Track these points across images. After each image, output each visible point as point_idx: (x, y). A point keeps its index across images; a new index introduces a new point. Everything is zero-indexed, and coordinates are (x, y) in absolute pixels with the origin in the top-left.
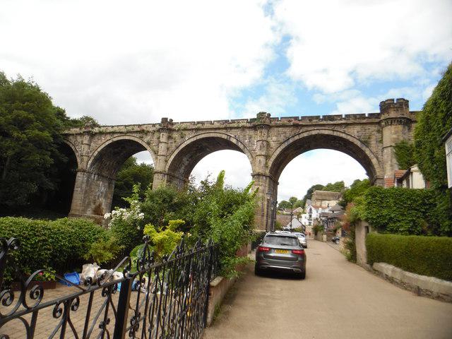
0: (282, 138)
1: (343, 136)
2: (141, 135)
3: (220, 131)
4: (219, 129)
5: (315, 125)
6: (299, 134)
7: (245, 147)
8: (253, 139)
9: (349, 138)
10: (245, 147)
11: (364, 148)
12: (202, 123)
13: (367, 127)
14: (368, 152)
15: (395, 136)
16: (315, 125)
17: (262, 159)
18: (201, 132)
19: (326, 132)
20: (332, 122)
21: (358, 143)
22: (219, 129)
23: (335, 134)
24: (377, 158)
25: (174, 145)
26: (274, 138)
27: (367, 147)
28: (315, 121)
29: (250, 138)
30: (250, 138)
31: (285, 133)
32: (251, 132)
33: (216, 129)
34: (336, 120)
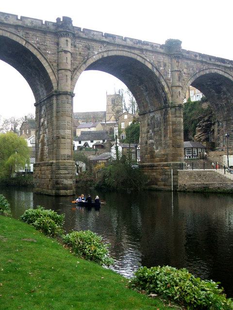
4: (134, 48)
6: (204, 70)
8: (167, 67)
12: (113, 37)
18: (111, 48)
23: (226, 75)
29: (165, 65)
30: (165, 65)
34: (226, 63)
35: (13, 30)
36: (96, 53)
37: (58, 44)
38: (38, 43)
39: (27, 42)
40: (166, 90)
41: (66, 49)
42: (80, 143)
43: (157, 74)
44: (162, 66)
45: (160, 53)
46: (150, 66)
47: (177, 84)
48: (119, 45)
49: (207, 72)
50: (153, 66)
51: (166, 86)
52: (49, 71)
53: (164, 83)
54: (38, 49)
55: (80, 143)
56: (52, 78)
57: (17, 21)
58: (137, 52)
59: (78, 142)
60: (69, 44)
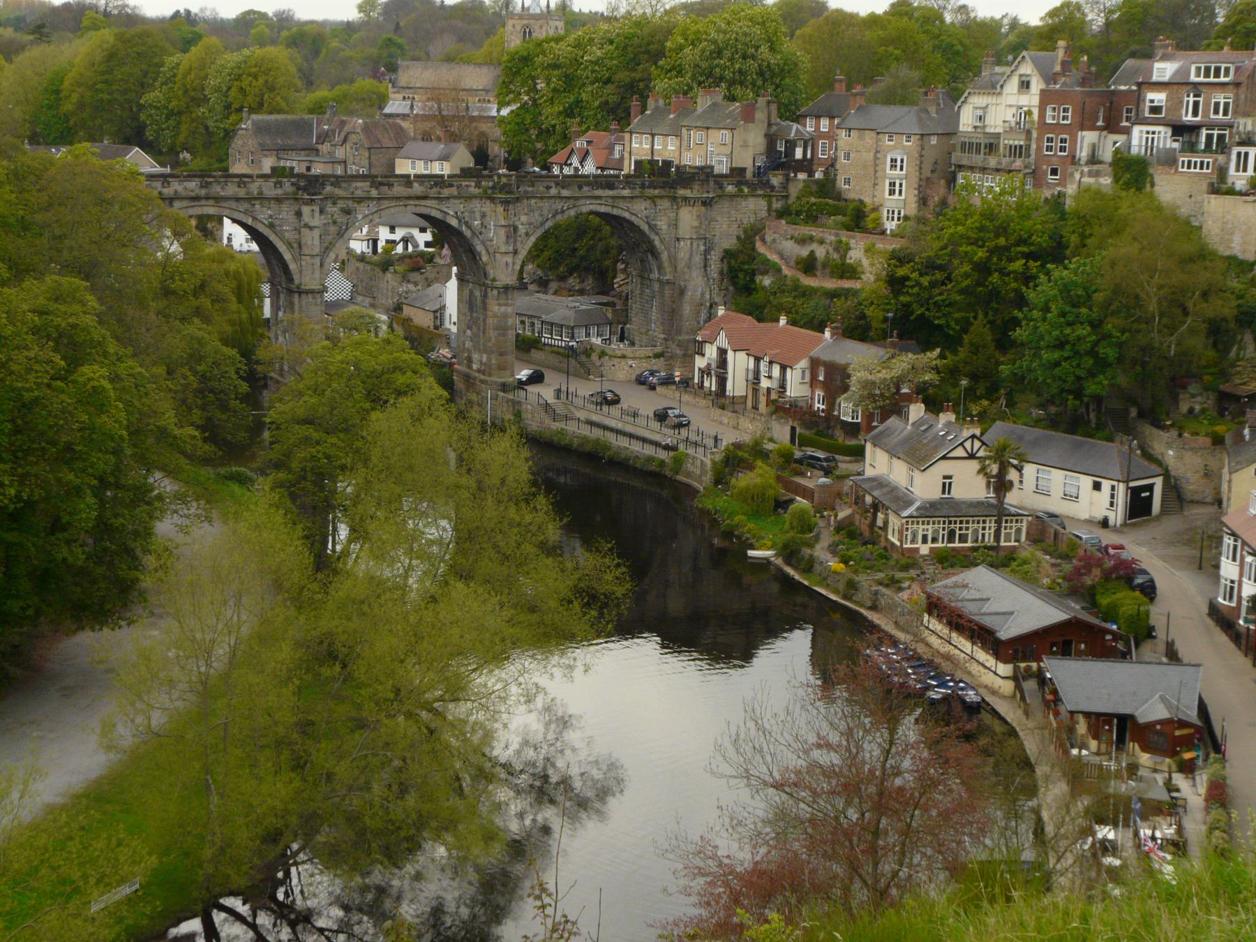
0: (536, 217)
1: (626, 215)
2: (246, 205)
3: (423, 202)
5: (587, 197)
6: (563, 212)
7: (474, 233)
9: (633, 219)
10: (474, 233)
11: (653, 236)
13: (659, 202)
14: (657, 243)
15: (696, 223)
16: (587, 197)
17: (509, 259)
19: (603, 209)
20: (611, 193)
21: (645, 227)
22: (425, 198)
23: (615, 212)
24: (668, 249)
25: (333, 229)
26: (524, 218)
27: (657, 234)
28: (585, 188)
29: (483, 216)
30: (483, 216)
31: (540, 208)
32: (487, 207)
33: (418, 198)
35: (233, 204)
36: (360, 217)
37: (299, 214)
38: (271, 217)
39: (254, 218)
40: (485, 258)
41: (312, 224)
42: (392, 230)
43: (468, 233)
44: (478, 216)
45: (475, 197)
46: (454, 222)
47: (503, 249)
48: (398, 198)
49: (572, 213)
50: (460, 221)
51: (484, 252)
52: (287, 256)
53: (479, 248)
54: (271, 226)
55: (392, 230)
56: (292, 266)
57: (237, 189)
58: (429, 203)
59: (387, 229)
60: (317, 214)
